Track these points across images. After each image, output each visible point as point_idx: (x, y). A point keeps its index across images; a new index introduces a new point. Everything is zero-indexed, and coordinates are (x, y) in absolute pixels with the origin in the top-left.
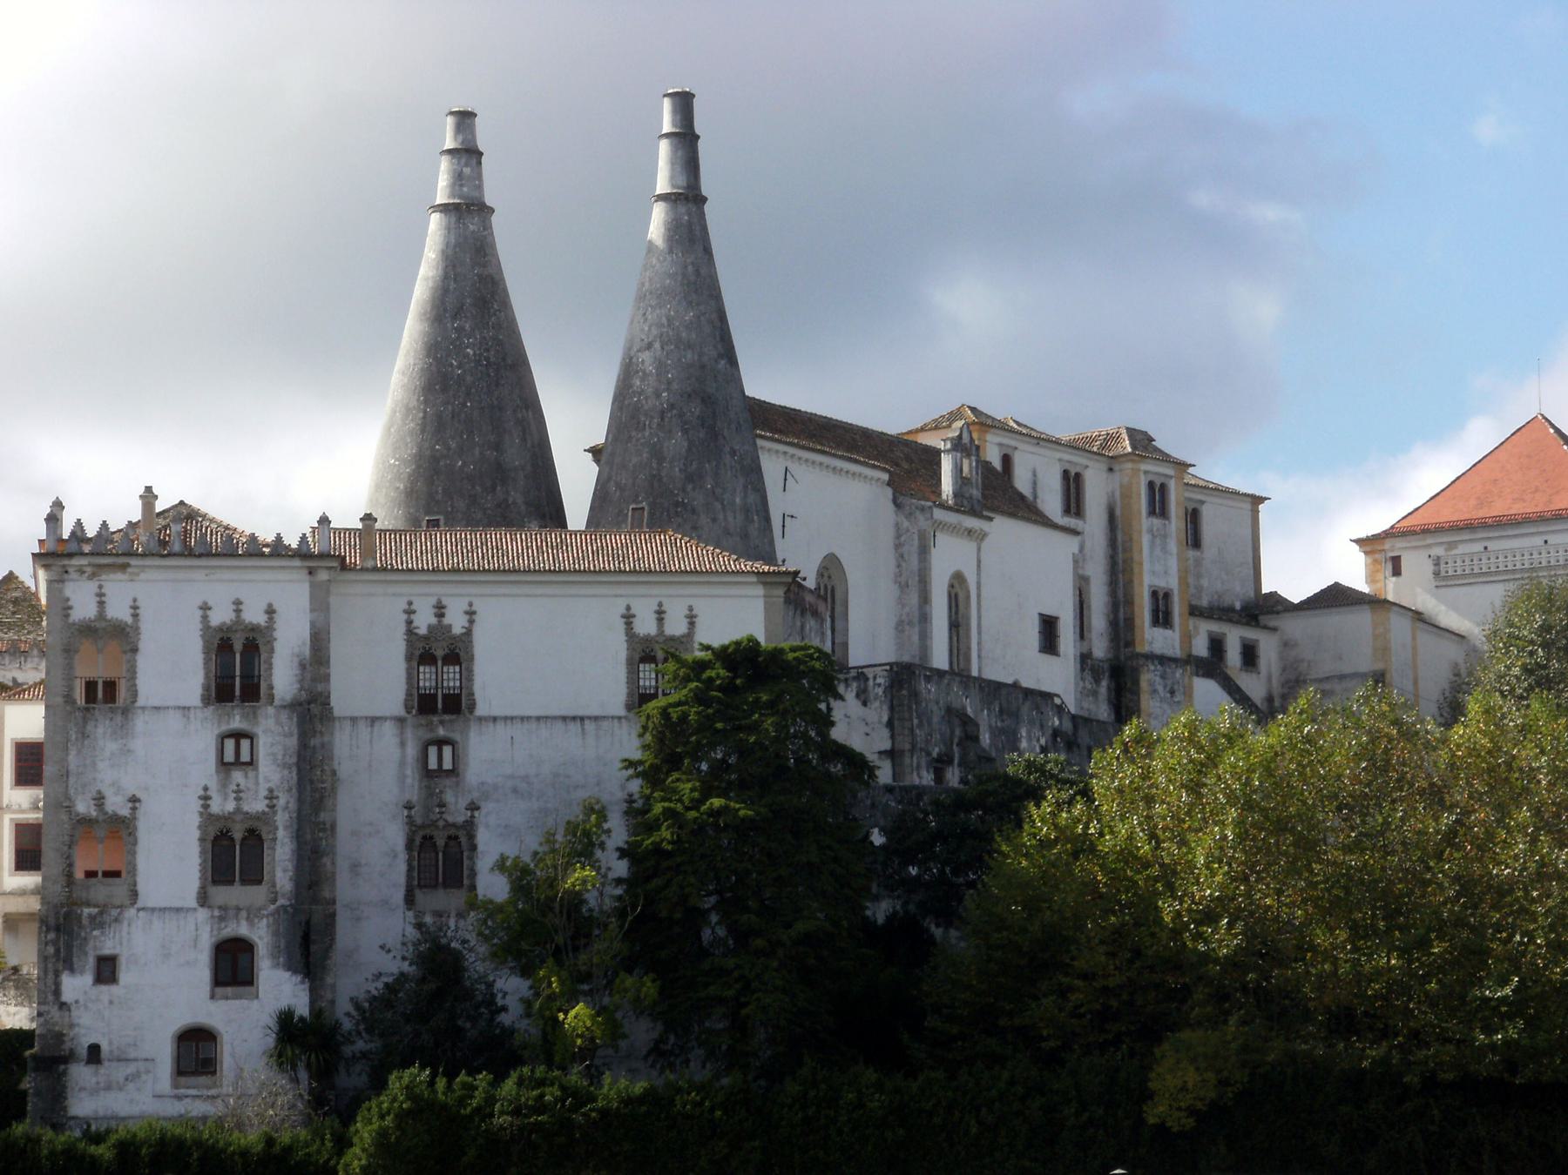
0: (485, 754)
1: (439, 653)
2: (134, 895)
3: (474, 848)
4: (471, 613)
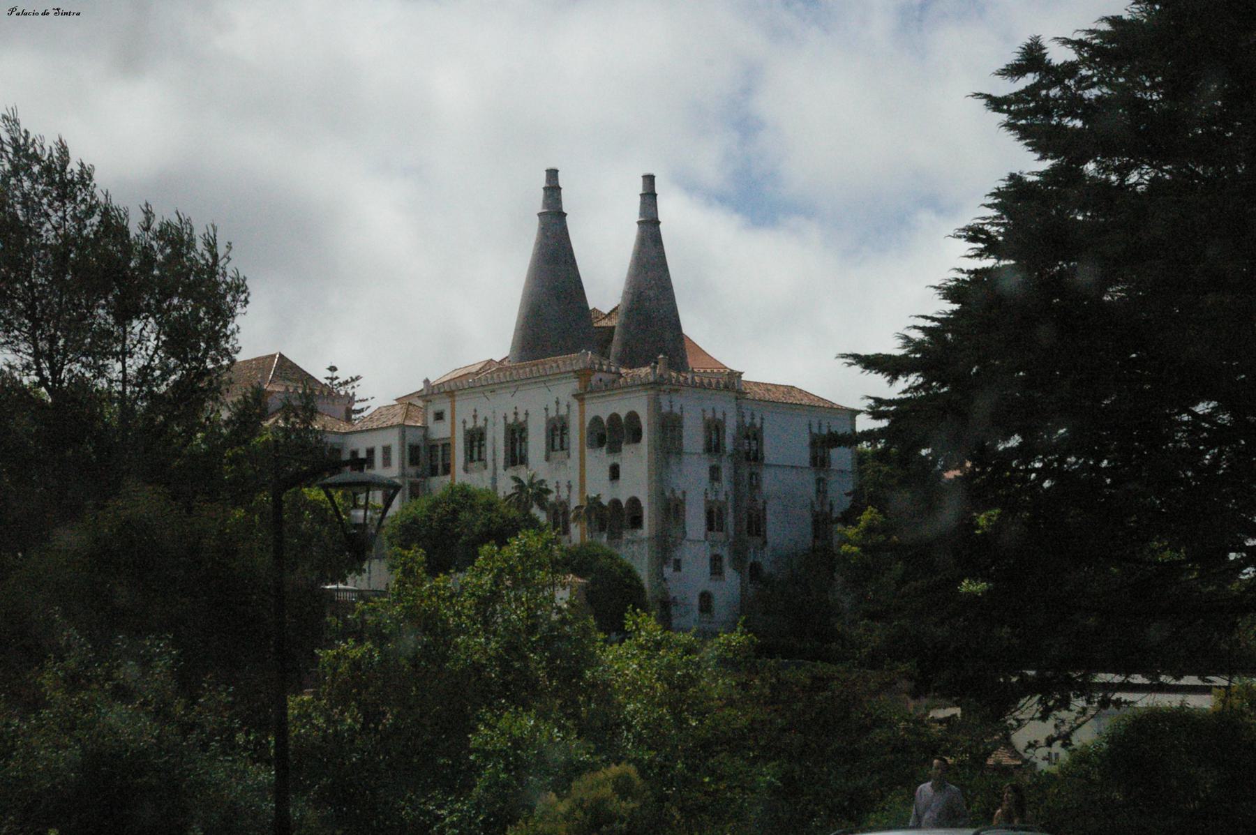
0: (770, 481)
2: (685, 532)
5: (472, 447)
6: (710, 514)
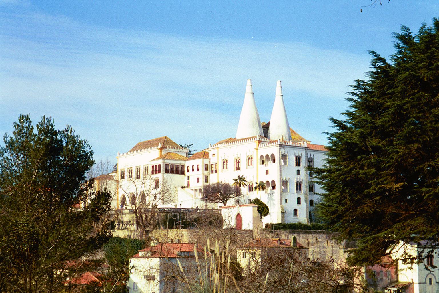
1: (310, 161)
3: (314, 187)
4: (313, 155)
5: (224, 165)
6: (297, 185)
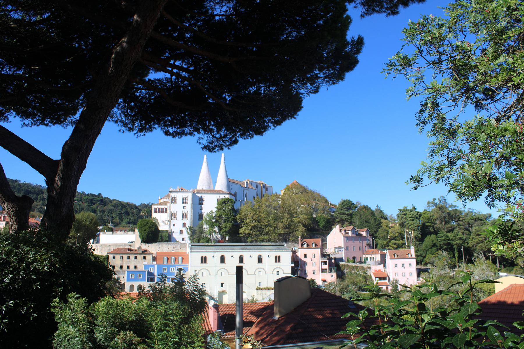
6: (183, 215)
